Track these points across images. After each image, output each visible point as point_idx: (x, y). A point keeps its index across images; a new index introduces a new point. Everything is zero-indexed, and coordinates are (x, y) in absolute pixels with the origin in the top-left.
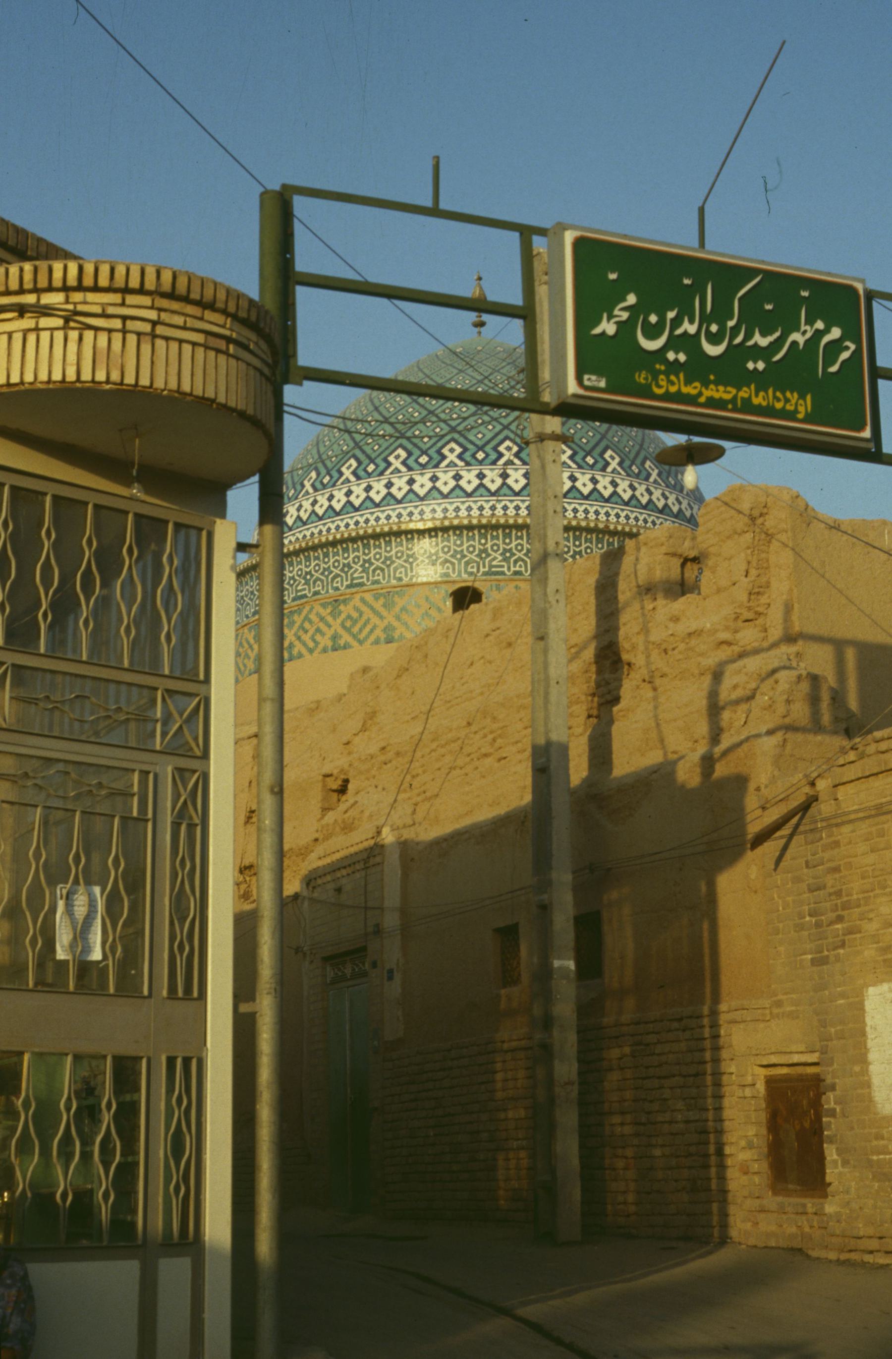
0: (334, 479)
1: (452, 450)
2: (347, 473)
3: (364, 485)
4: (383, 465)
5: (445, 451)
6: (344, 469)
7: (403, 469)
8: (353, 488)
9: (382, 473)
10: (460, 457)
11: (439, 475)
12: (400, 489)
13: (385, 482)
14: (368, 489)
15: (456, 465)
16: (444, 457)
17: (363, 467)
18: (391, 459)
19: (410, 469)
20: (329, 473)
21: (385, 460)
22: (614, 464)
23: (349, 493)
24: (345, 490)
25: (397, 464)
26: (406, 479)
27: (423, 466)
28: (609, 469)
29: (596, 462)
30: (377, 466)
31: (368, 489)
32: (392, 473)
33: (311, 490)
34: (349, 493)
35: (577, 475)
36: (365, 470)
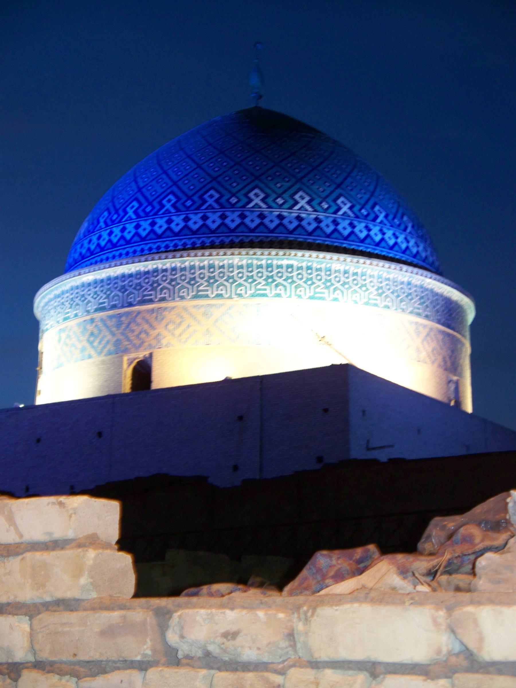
0: (155, 210)
1: (257, 195)
2: (168, 206)
3: (183, 217)
4: (199, 202)
5: (251, 195)
6: (164, 202)
7: (216, 205)
8: (174, 218)
9: (198, 208)
10: (263, 200)
11: (247, 213)
12: (214, 222)
13: (200, 215)
14: (187, 219)
15: (260, 207)
16: (251, 201)
17: (182, 201)
18: (206, 196)
19: (222, 206)
20: (150, 203)
21: (201, 197)
22: (381, 217)
23: (169, 221)
24: (165, 219)
25: (211, 201)
26: (219, 214)
27: (233, 206)
28: (378, 220)
29: (368, 215)
30: (194, 202)
31: (187, 219)
32: (206, 209)
33: (134, 217)
34: (169, 221)
35: (356, 223)
36: (183, 204)
